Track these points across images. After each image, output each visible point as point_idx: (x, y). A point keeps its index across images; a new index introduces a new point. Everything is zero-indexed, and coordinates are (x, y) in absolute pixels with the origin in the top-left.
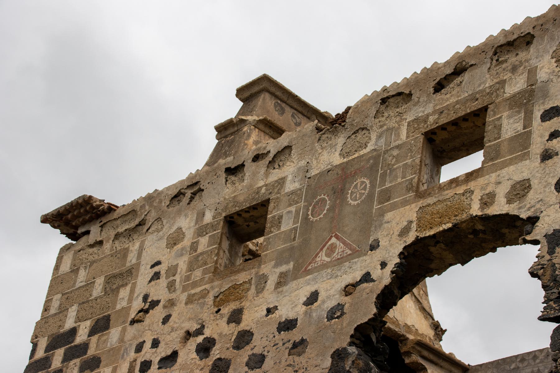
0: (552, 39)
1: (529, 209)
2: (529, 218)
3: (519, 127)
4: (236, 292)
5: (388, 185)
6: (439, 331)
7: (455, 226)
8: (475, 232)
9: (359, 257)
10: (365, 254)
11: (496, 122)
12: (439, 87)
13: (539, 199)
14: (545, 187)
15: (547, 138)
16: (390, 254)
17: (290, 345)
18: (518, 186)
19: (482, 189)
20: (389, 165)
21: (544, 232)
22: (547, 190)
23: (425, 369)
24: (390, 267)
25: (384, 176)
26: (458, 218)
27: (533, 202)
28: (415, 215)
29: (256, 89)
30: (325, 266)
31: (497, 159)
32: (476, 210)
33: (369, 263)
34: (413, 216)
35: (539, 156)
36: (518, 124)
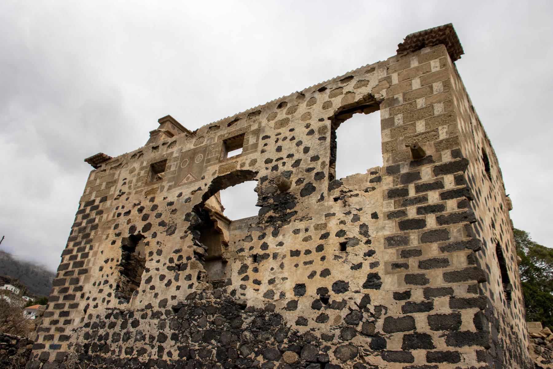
0: (267, 113)
3: (255, 141)
4: (153, 191)
5: (209, 157)
6: (223, 209)
7: (231, 173)
8: (238, 176)
12: (229, 125)
17: (171, 211)
19: (241, 161)
23: (217, 221)
24: (208, 186)
25: (208, 154)
29: (165, 120)
30: (185, 184)
32: (238, 168)
33: (201, 184)
34: (217, 169)
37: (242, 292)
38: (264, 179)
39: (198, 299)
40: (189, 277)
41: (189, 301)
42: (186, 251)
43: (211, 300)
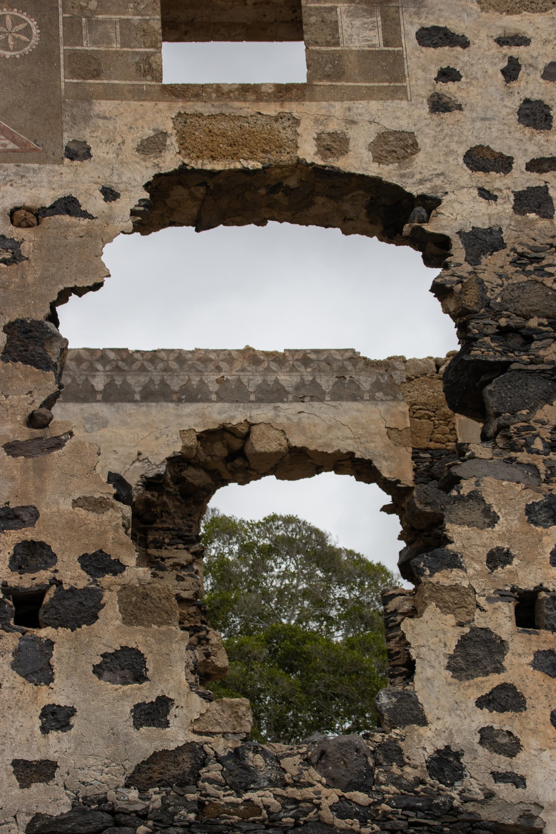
1: (421, 182)
2: (423, 197)
3: (376, 38)
9: (42, 161)
10: (60, 162)
11: (325, 15)
13: (438, 171)
14: (446, 154)
15: (436, 76)
16: (124, 179)
18: (392, 139)
20: (82, 8)
21: (457, 226)
22: (451, 159)
25: (73, 25)
26: (269, 156)
27: (426, 174)
28: (171, 125)
31: (339, 79)
32: (308, 152)
35: (425, 101)
36: (372, 33)
37: (502, 763)
38: (482, 242)
39: (222, 785)
40: (126, 665)
41: (156, 797)
42: (71, 525)
43: (309, 792)
